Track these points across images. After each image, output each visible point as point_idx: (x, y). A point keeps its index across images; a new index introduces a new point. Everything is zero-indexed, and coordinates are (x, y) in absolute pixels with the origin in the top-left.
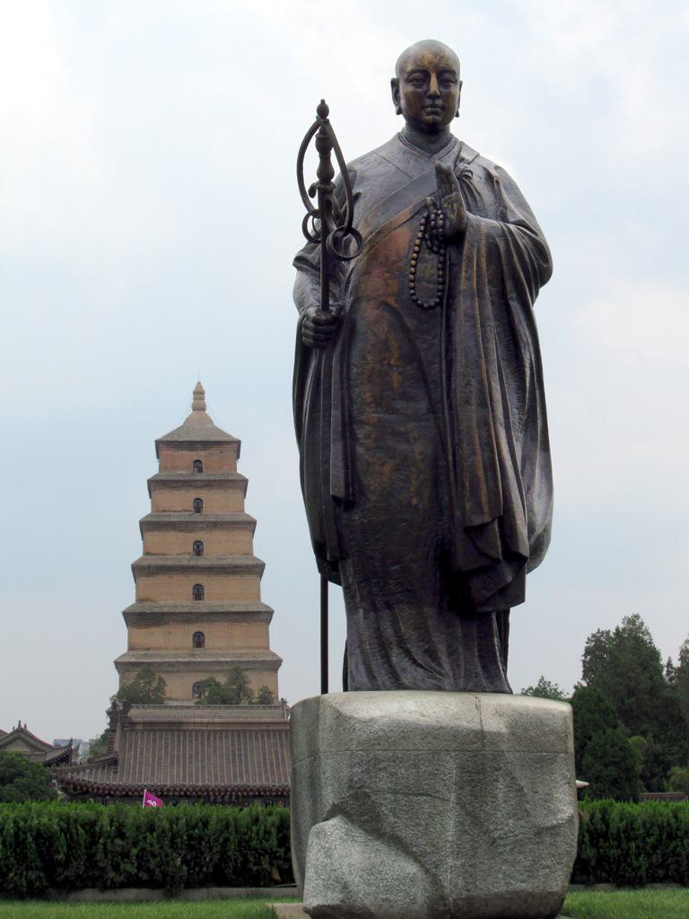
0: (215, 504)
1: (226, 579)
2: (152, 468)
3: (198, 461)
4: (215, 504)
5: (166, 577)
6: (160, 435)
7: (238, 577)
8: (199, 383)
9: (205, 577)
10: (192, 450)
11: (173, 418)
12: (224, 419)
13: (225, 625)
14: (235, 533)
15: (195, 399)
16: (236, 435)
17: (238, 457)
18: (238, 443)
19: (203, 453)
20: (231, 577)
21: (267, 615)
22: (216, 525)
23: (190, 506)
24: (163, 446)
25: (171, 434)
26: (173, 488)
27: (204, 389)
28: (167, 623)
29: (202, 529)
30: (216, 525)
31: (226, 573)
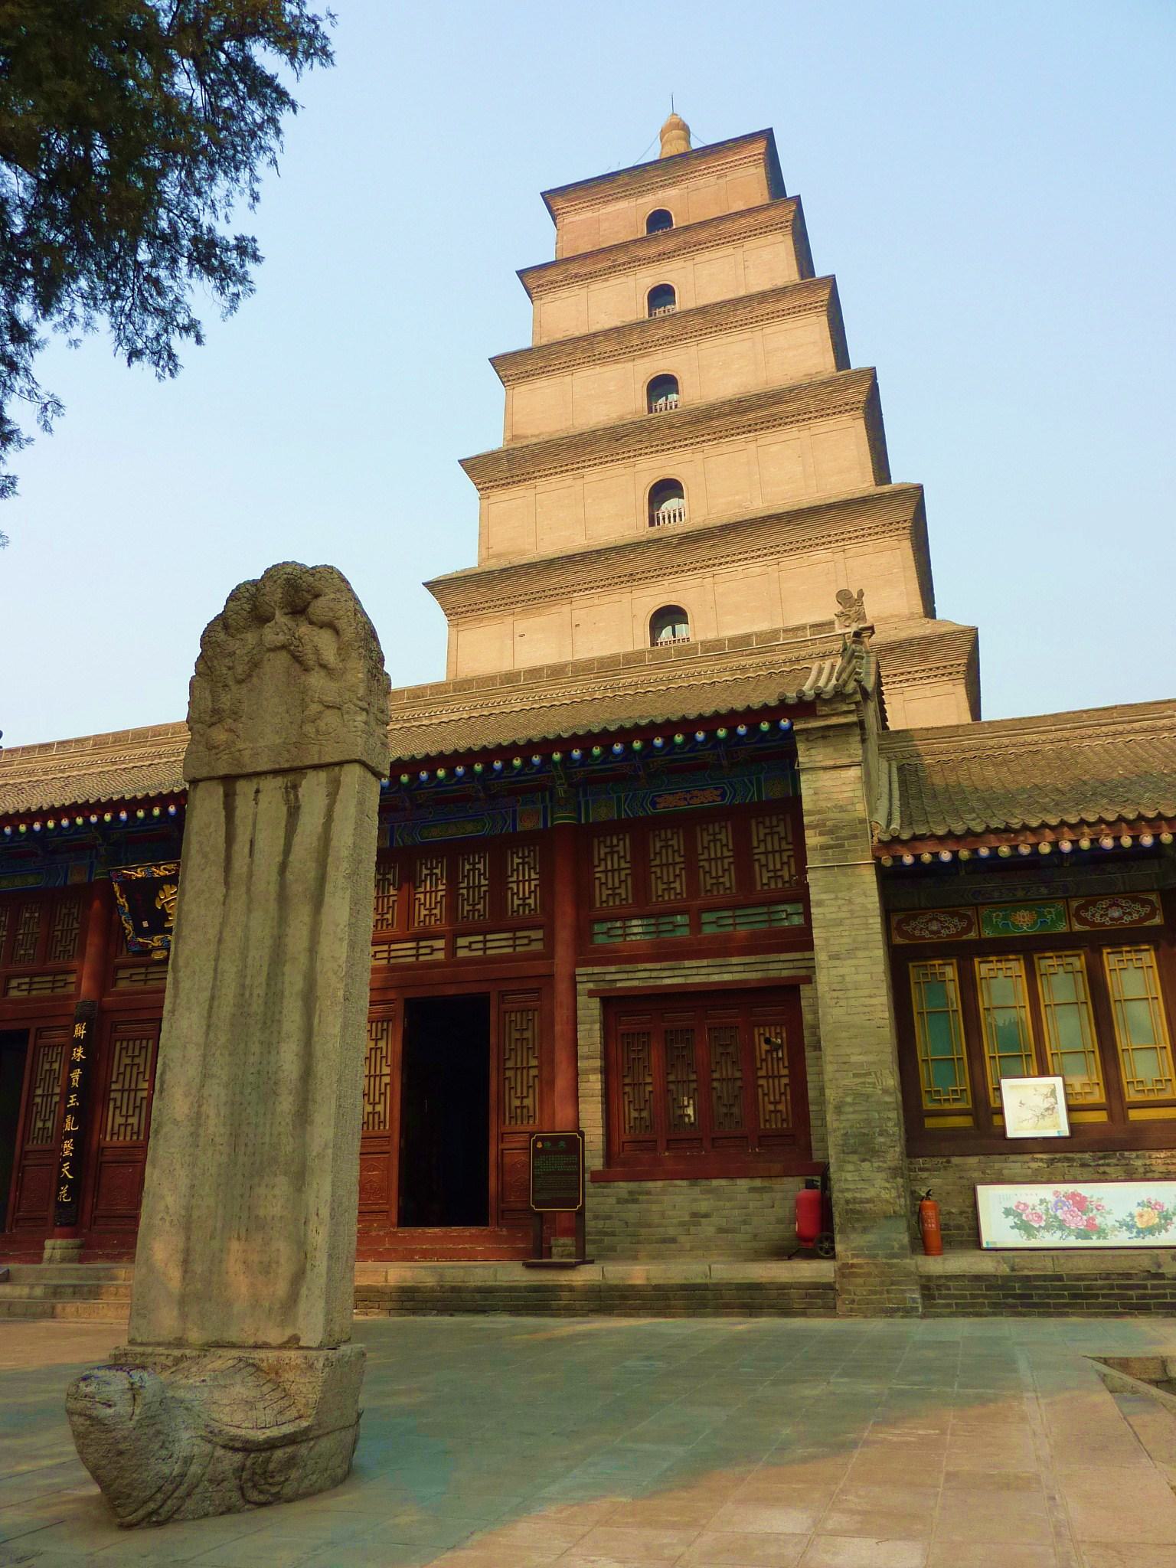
1: (752, 446)
5: (567, 480)
7: (792, 432)
9: (685, 455)
10: (641, 194)
13: (756, 568)
14: (767, 331)
18: (768, 135)
19: (673, 192)
20: (767, 438)
22: (715, 317)
23: (639, 310)
26: (592, 276)
28: (563, 594)
29: (671, 340)
30: (715, 317)
31: (751, 429)
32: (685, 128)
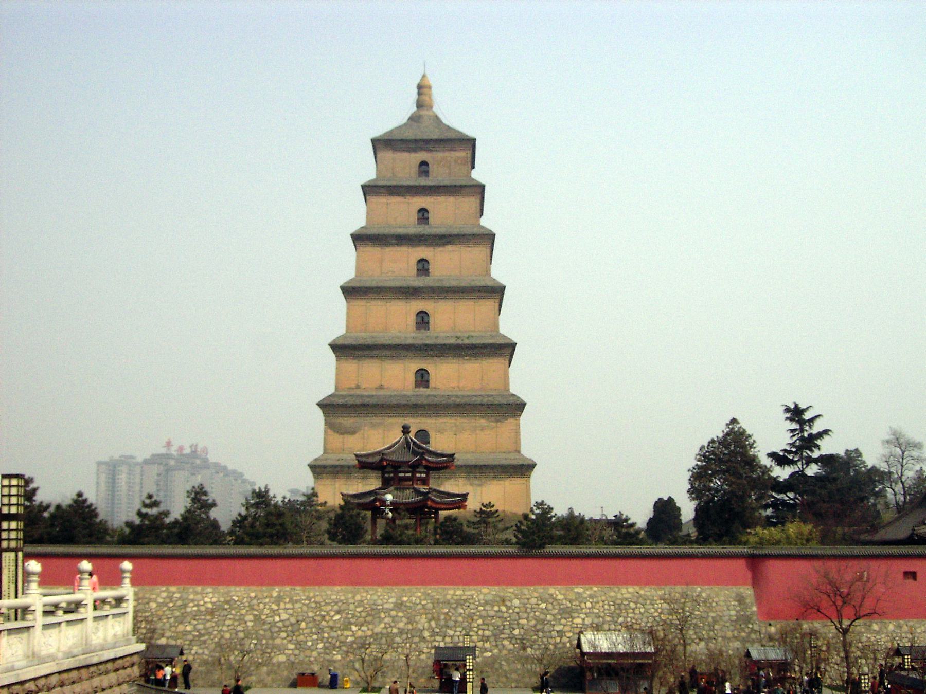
0: (446, 212)
2: (367, 169)
3: (424, 164)
4: (446, 212)
6: (380, 130)
8: (424, 76)
11: (395, 115)
12: (454, 114)
15: (419, 94)
16: (469, 132)
17: (473, 167)
18: (474, 140)
21: (506, 349)
24: (381, 144)
25: (391, 132)
27: (432, 80)
32: (430, 87)
